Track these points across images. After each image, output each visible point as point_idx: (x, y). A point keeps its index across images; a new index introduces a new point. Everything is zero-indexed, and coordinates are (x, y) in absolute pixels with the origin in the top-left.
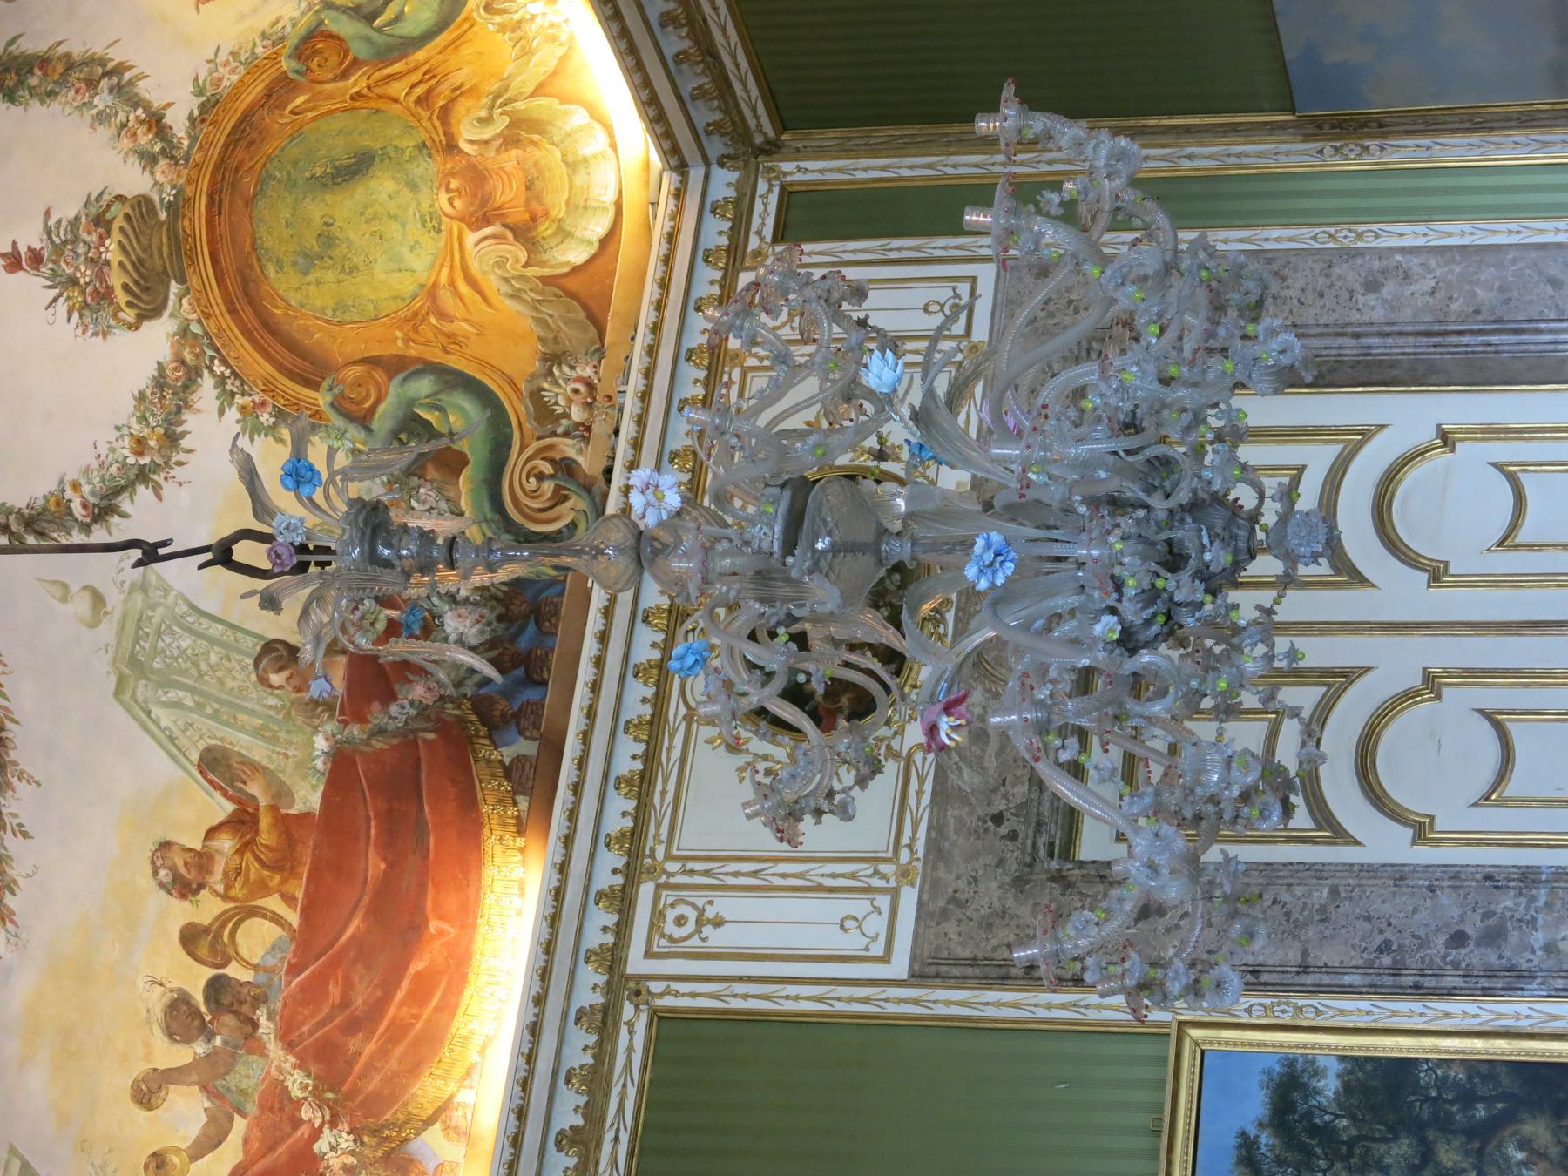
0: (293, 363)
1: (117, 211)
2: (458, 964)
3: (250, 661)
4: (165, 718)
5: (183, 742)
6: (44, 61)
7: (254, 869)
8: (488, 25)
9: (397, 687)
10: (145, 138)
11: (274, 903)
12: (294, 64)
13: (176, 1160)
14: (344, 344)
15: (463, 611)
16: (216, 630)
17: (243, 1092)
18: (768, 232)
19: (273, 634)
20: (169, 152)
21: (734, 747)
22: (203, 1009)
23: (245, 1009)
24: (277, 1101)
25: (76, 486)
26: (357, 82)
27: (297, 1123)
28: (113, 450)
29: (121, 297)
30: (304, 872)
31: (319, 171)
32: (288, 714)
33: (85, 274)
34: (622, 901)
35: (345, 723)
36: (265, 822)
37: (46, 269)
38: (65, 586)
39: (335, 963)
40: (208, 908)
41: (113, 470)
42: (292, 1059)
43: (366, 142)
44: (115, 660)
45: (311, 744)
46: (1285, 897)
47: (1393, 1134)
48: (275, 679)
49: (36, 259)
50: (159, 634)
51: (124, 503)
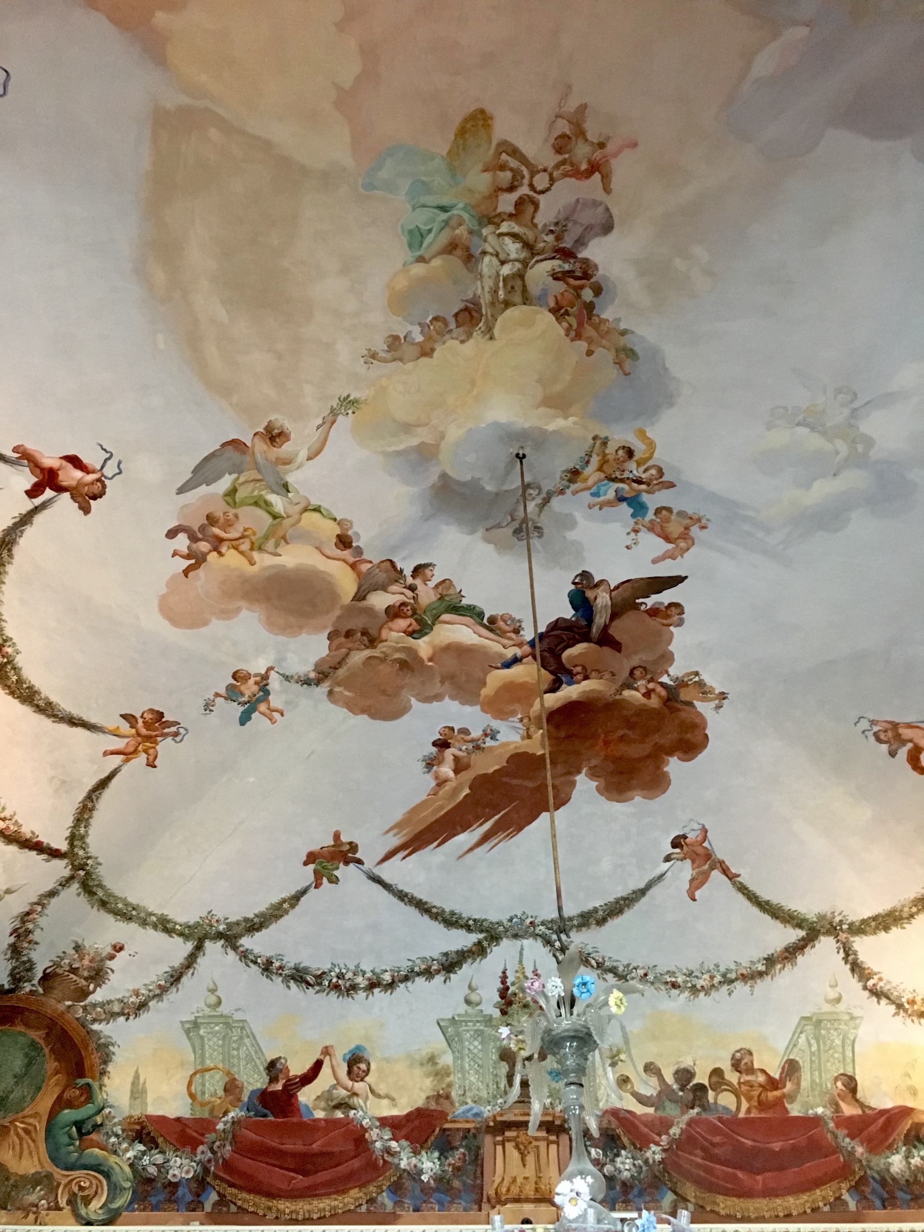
3: (842, 1071)
4: (802, 1040)
5: (795, 1050)
9: (858, 1139)
11: (745, 1105)
13: (629, 1086)
15: (904, 1163)
16: (849, 1054)
17: (664, 1108)
19: (857, 1078)
22: (691, 1084)
23: (698, 1102)
24: (664, 1125)
25: (880, 979)
27: (660, 1135)
28: (904, 991)
30: (763, 1115)
32: (826, 1093)
35: (832, 1119)
36: (777, 1093)
38: (837, 985)
39: (726, 1136)
41: (896, 993)
42: (684, 1126)
44: (815, 1013)
45: (818, 1106)
48: (839, 1084)
50: (836, 1029)
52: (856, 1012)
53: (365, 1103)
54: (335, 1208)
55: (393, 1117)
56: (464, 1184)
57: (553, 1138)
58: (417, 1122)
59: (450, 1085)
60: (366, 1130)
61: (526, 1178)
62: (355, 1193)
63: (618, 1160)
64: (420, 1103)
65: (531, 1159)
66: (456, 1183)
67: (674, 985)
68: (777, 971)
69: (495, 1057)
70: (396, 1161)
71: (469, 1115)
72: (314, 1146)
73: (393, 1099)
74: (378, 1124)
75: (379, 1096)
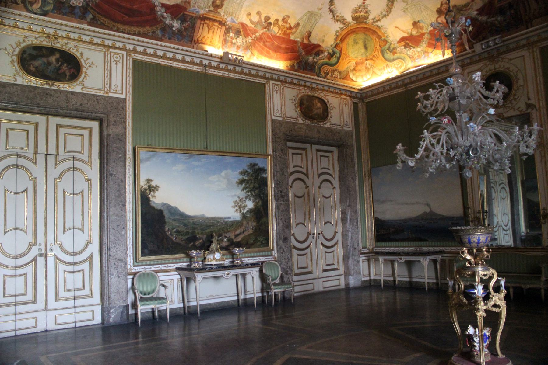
0: (341, 39)
2: (271, 57)
4: (304, 18)
6: (392, 5)
7: (284, 29)
8: (385, 65)
10: (377, 19)
11: (280, 32)
14: (344, 45)
20: (374, 22)
21: (297, 96)
24: (256, 32)
26: (378, 47)
33: (360, 10)
34: (278, 80)
36: (290, 31)
40: (280, 23)
43: (369, 49)
47: (258, 184)
49: (364, 3)
51: (331, 14)
52: (323, 14)
54: (140, 31)
55: (167, 5)
56: (187, 34)
57: (220, 26)
58: (175, 9)
60: (155, 6)
62: (148, 28)
63: (238, 39)
65: (211, 31)
66: (184, 33)
70: (164, 20)
71: (195, 11)
72: (134, 7)
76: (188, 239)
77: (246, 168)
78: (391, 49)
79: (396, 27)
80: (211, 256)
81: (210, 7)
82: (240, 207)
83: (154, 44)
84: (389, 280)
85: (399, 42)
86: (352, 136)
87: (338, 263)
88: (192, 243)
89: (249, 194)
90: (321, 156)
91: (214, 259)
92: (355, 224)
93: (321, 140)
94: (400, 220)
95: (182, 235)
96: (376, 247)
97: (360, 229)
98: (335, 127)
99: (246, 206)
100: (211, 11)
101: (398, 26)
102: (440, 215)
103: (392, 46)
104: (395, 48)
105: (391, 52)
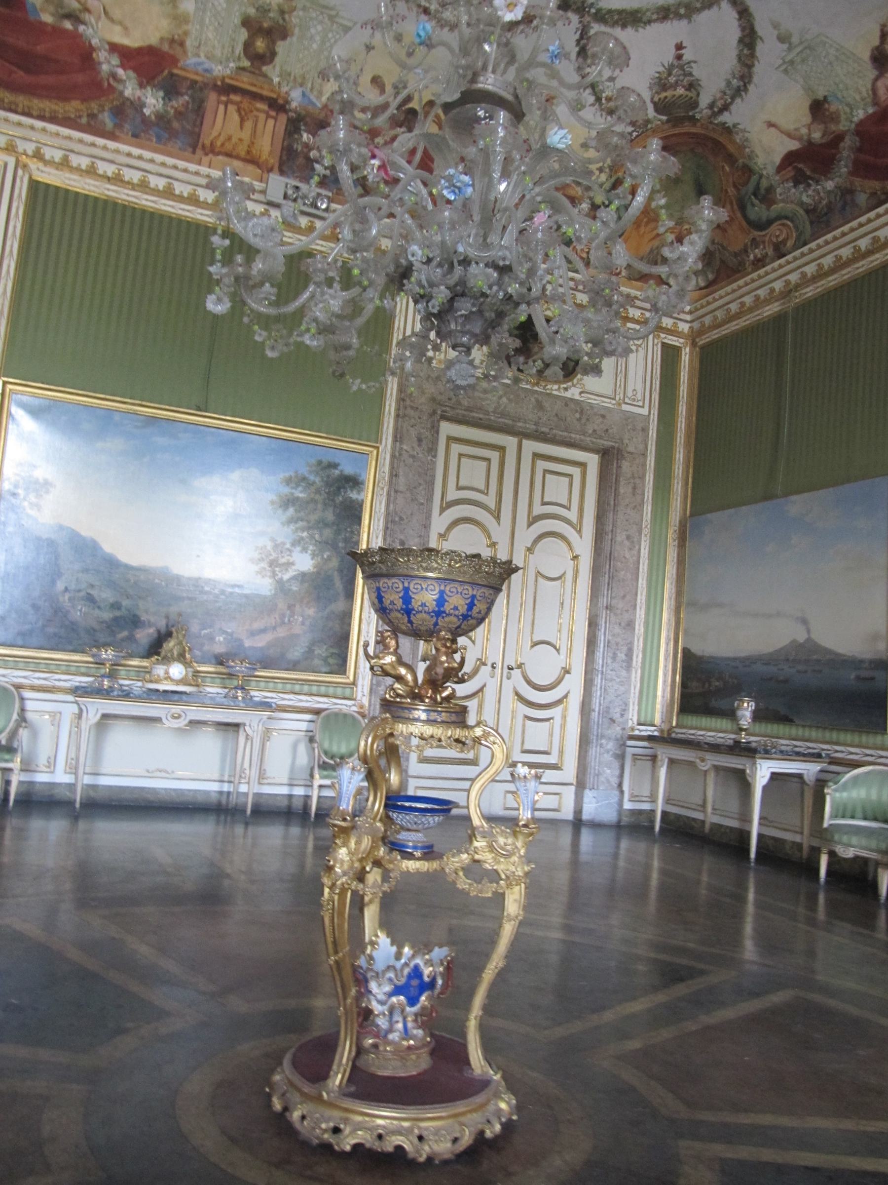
1: (692, 94)
6: (752, 55)
10: (719, 104)
12: (741, 165)
18: (665, 341)
20: (715, 115)
22: (407, 107)
23: (406, 124)
26: (731, 191)
29: (663, 95)
31: (701, 178)
33: (672, 79)
37: (676, 63)
41: (601, 87)
46: (421, 488)
49: (679, 57)
53: (97, 23)
54: (55, 112)
57: (273, 113)
59: (186, 33)
60: (92, 49)
61: (241, 140)
62: (76, 104)
64: (153, 39)
65: (248, 125)
66: (176, 125)
67: (426, 11)
68: (519, 31)
69: (237, 21)
70: (120, 87)
72: (38, 48)
73: (126, 28)
74: (107, 47)
75: (112, 20)
76: (116, 619)
77: (304, 471)
78: (762, 191)
79: (771, 125)
80: (160, 670)
81: (239, 59)
82: (273, 564)
83: (86, 144)
84: (694, 819)
85: (780, 168)
86: (645, 430)
87: (561, 752)
88: (125, 633)
89: (305, 534)
90: (546, 471)
91: (168, 678)
92: (621, 656)
93: (544, 429)
94: (735, 659)
95: (99, 607)
96: (677, 726)
97: (636, 676)
98: (594, 400)
99: (293, 564)
100: (243, 69)
101: (773, 120)
102: (828, 651)
103: (764, 183)
104: (770, 189)
105: (761, 201)
